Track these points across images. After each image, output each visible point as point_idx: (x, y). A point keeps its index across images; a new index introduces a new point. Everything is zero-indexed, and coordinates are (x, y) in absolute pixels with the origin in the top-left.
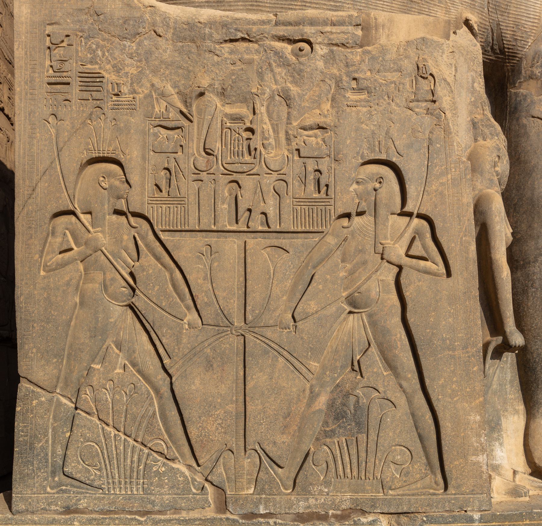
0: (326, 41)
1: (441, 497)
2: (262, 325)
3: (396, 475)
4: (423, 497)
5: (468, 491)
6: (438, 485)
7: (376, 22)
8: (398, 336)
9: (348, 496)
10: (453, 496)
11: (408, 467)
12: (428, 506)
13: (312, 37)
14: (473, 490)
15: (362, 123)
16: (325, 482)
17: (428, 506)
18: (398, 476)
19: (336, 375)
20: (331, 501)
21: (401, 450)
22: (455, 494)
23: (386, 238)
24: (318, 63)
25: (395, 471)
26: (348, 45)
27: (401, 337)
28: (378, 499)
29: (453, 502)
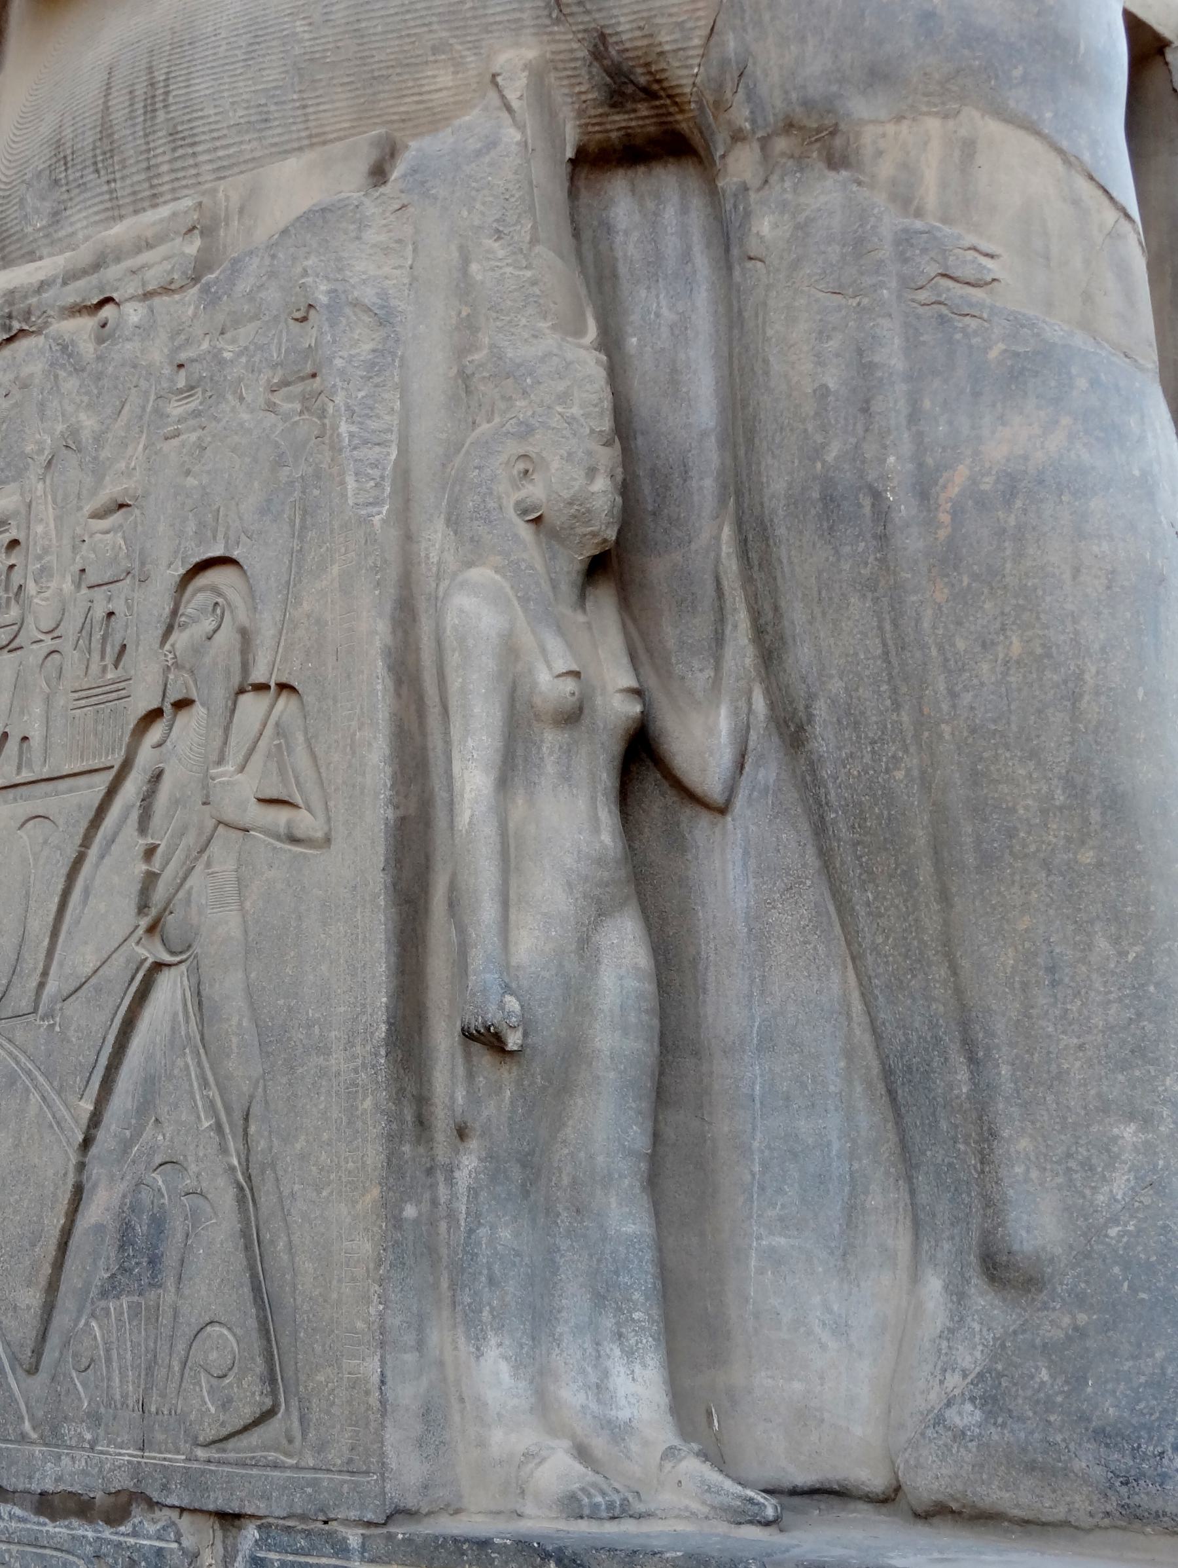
0: (140, 292)
1: (288, 1474)
2: (10, 1014)
3: (210, 1405)
4: (255, 1472)
5: (339, 1462)
6: (290, 1441)
7: (227, 207)
8: (235, 1021)
9: (128, 1455)
10: (310, 1475)
11: (230, 1385)
12: (262, 1497)
13: (117, 290)
14: (350, 1461)
15: (188, 473)
16: (89, 1415)
17: (262, 1497)
18: (213, 1410)
19: (128, 1133)
20: (96, 1465)
21: (221, 1335)
22: (315, 1469)
23: (220, 761)
24: (128, 346)
25: (209, 1393)
26: (173, 287)
27: (240, 1024)
28: (175, 1469)
29: (309, 1490)
